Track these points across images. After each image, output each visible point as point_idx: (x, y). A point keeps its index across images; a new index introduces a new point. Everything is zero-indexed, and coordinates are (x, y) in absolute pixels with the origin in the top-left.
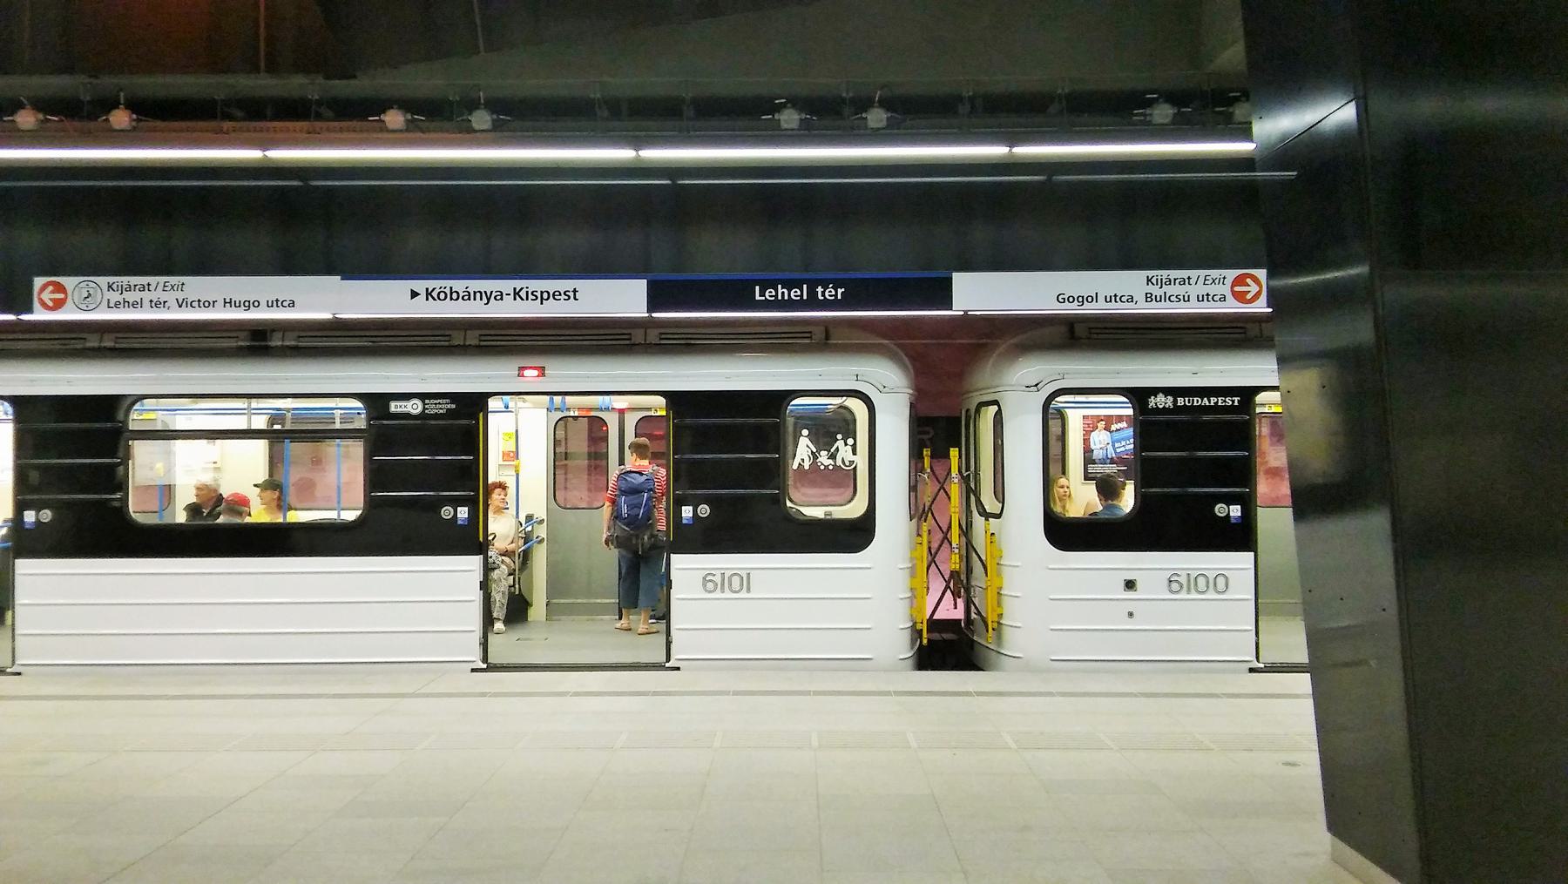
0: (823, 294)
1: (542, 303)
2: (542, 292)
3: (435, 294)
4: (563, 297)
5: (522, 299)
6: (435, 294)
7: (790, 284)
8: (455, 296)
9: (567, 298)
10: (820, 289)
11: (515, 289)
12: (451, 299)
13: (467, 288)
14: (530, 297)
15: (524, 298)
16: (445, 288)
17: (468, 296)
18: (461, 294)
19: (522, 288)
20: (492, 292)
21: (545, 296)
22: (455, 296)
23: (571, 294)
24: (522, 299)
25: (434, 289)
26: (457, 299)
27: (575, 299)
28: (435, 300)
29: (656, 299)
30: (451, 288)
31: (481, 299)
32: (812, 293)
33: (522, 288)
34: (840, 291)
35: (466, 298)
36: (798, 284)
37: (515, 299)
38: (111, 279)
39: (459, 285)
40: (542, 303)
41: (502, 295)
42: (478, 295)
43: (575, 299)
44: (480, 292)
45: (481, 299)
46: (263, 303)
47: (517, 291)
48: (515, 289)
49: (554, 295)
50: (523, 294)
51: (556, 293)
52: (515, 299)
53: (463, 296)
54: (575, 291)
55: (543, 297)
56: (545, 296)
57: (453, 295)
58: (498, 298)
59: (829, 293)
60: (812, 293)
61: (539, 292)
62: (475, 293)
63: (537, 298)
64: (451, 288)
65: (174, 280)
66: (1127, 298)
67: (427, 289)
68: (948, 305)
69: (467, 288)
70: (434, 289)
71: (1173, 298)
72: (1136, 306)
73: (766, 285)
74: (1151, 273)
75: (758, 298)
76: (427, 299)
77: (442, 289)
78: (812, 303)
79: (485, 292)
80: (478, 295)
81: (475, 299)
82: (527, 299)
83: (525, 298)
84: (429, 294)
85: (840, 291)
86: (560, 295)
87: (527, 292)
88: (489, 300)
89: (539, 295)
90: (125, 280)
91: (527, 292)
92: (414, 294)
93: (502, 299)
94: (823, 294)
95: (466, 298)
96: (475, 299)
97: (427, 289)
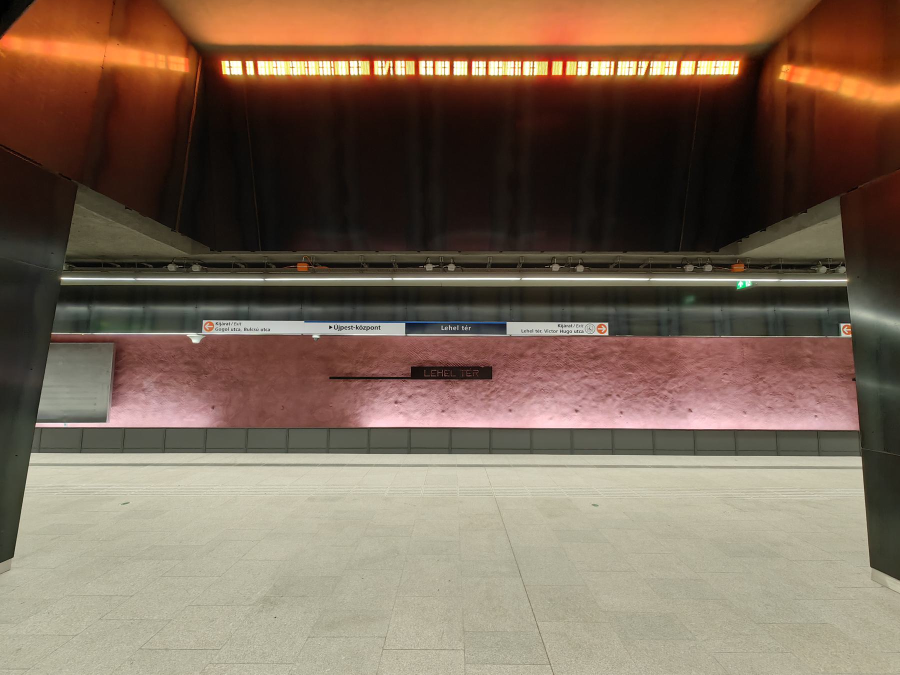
0: (464, 328)
7: (453, 325)
10: (463, 327)
21: (368, 328)
29: (410, 328)
32: (460, 328)
34: (470, 328)
36: (455, 325)
38: (217, 321)
46: (260, 330)
54: (379, 327)
55: (368, 328)
56: (368, 328)
59: (466, 328)
60: (460, 328)
65: (238, 322)
68: (506, 334)
71: (253, 330)
73: (445, 325)
74: (559, 323)
75: (442, 329)
78: (460, 331)
85: (470, 328)
90: (222, 321)
94: (464, 328)
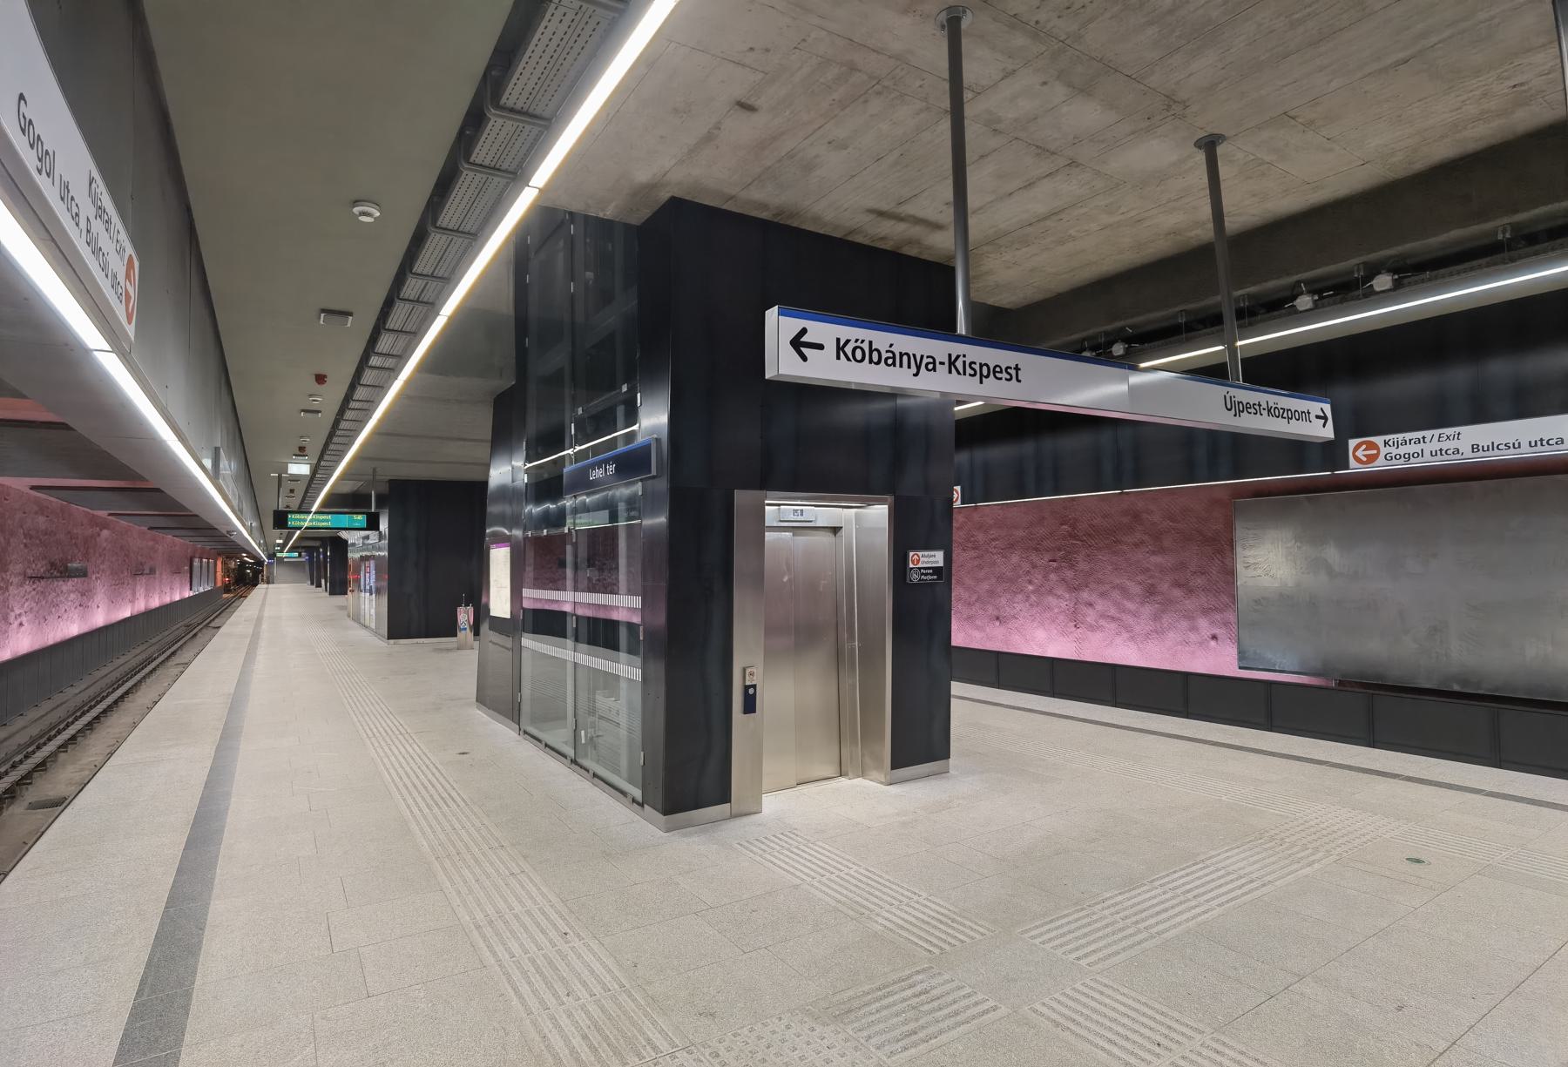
1: (981, 382)
2: (981, 366)
3: (848, 349)
4: (1005, 375)
6: (848, 349)
8: (875, 357)
9: (1008, 377)
11: (950, 355)
12: (871, 361)
13: (891, 346)
14: (969, 371)
15: (961, 371)
16: (863, 341)
17: (894, 360)
18: (884, 356)
19: (958, 357)
20: (922, 357)
22: (875, 357)
23: (1013, 372)
24: (959, 373)
25: (848, 341)
26: (878, 363)
27: (1019, 381)
28: (848, 359)
30: (871, 343)
31: (909, 367)
33: (958, 357)
35: (890, 361)
37: (950, 372)
39: (882, 339)
40: (981, 382)
41: (934, 363)
42: (905, 358)
43: (1019, 381)
44: (907, 354)
45: (909, 367)
47: (953, 359)
48: (950, 355)
49: (995, 372)
50: (959, 364)
51: (998, 369)
52: (950, 372)
53: (886, 359)
57: (872, 355)
58: (930, 366)
61: (978, 365)
62: (901, 355)
63: (975, 371)
64: (871, 343)
66: (1452, 451)
67: (838, 340)
69: (891, 346)
70: (848, 341)
72: (1462, 457)
76: (838, 358)
77: (858, 344)
79: (914, 355)
80: (905, 358)
81: (901, 366)
82: (965, 374)
83: (961, 371)
84: (840, 349)
86: (1001, 372)
87: (964, 362)
88: (918, 368)
89: (977, 367)
91: (964, 362)
93: (934, 369)
95: (890, 361)
96: (901, 366)
97: (838, 340)
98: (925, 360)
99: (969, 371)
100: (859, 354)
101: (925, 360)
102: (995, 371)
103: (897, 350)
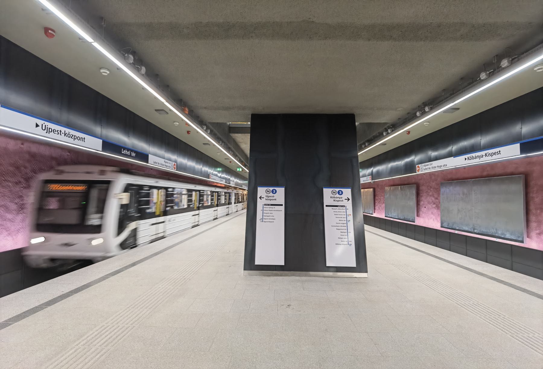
2: (492, 153)
5: (487, 156)
6: (469, 158)
14: (489, 155)
17: (476, 158)
23: (499, 152)
24: (487, 156)
49: (495, 154)
50: (487, 155)
54: (500, 151)
55: (492, 155)
57: (473, 158)
88: (480, 158)
89: (491, 154)
92: (466, 159)
98: (481, 156)
99: (489, 155)
100: (471, 158)
101: (481, 156)
102: (495, 154)
103: (476, 156)
